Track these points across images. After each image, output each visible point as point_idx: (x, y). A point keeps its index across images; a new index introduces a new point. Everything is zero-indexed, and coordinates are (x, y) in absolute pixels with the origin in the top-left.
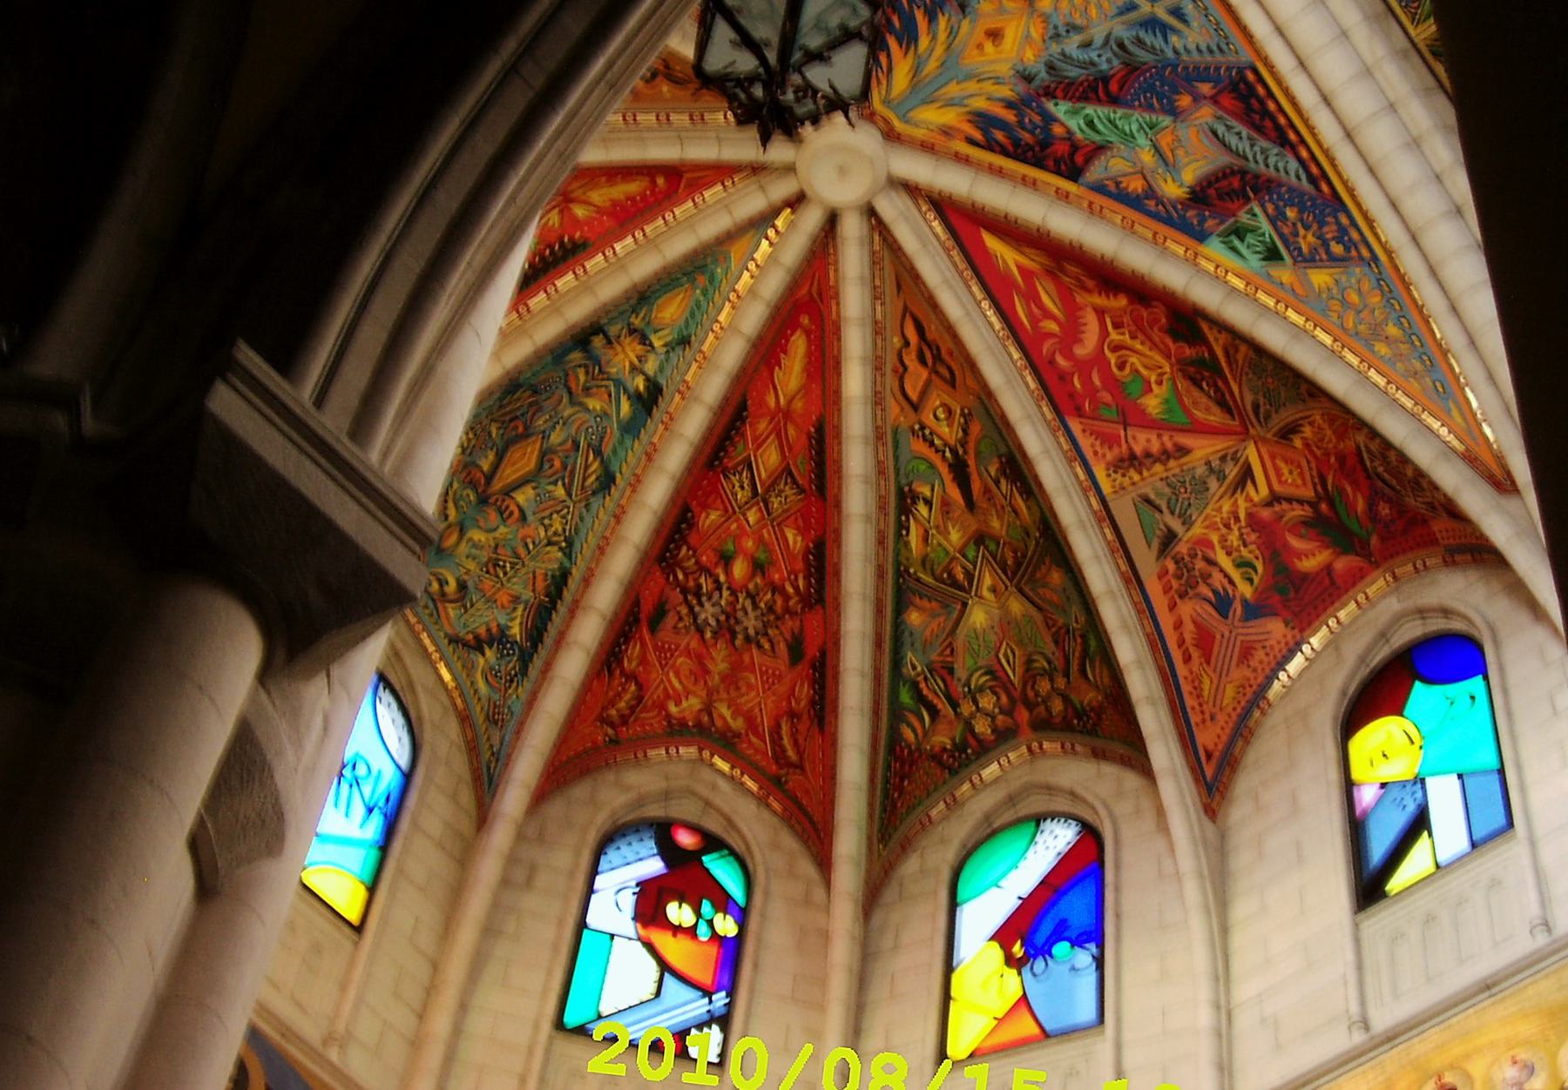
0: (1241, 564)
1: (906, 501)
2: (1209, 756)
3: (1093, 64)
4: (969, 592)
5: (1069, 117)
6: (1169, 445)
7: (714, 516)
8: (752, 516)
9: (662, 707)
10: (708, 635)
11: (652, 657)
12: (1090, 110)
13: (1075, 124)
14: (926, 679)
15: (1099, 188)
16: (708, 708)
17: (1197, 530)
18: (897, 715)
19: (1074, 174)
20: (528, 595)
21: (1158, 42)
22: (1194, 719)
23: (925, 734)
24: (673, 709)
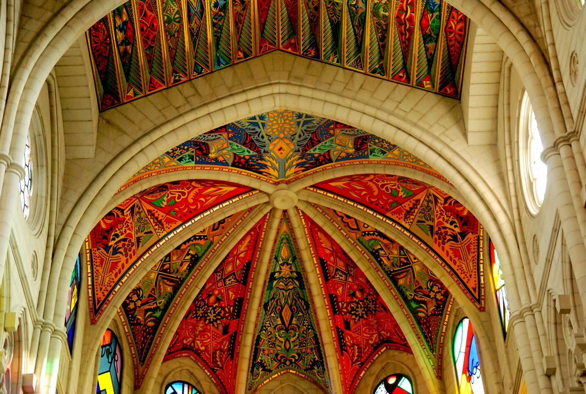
0: (451, 223)
1: (375, 254)
2: (475, 290)
3: (307, 138)
4: (410, 264)
5: (316, 151)
6: (414, 202)
7: (340, 289)
8: (350, 280)
9: (367, 344)
10: (366, 317)
11: (354, 335)
12: (317, 147)
13: (317, 151)
14: (417, 296)
15: (337, 160)
16: (380, 335)
17: (436, 221)
18: (415, 312)
19: (331, 161)
20: (313, 346)
21: (313, 125)
22: (465, 281)
23: (427, 311)
24: (371, 342)
